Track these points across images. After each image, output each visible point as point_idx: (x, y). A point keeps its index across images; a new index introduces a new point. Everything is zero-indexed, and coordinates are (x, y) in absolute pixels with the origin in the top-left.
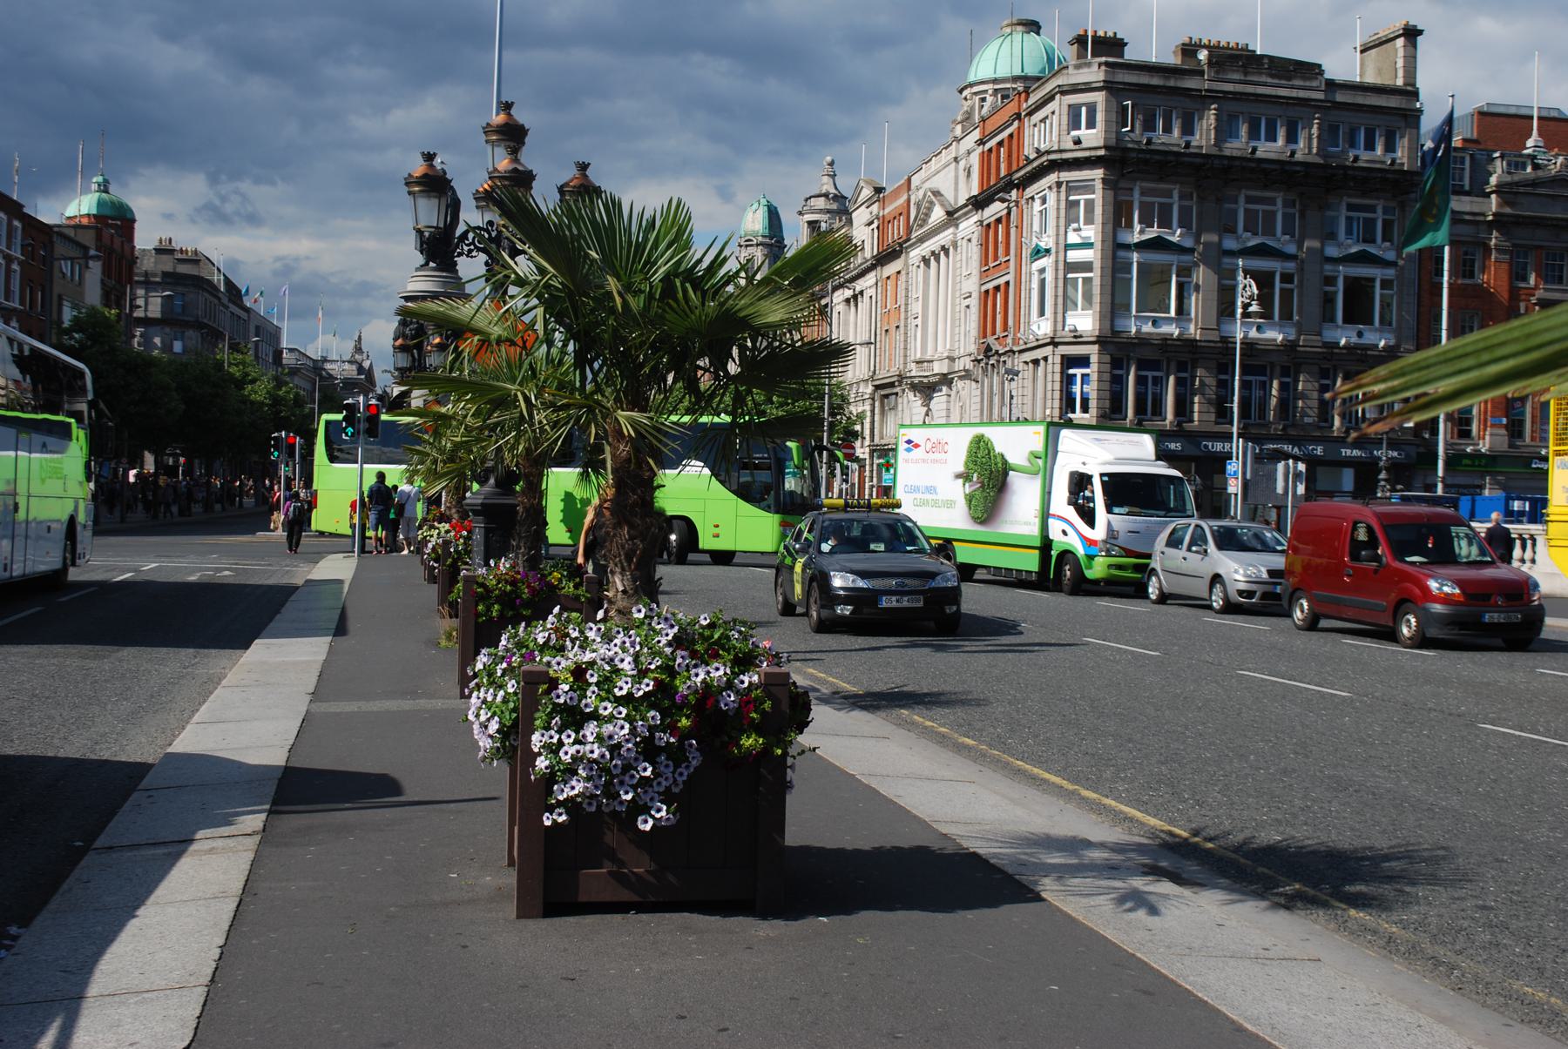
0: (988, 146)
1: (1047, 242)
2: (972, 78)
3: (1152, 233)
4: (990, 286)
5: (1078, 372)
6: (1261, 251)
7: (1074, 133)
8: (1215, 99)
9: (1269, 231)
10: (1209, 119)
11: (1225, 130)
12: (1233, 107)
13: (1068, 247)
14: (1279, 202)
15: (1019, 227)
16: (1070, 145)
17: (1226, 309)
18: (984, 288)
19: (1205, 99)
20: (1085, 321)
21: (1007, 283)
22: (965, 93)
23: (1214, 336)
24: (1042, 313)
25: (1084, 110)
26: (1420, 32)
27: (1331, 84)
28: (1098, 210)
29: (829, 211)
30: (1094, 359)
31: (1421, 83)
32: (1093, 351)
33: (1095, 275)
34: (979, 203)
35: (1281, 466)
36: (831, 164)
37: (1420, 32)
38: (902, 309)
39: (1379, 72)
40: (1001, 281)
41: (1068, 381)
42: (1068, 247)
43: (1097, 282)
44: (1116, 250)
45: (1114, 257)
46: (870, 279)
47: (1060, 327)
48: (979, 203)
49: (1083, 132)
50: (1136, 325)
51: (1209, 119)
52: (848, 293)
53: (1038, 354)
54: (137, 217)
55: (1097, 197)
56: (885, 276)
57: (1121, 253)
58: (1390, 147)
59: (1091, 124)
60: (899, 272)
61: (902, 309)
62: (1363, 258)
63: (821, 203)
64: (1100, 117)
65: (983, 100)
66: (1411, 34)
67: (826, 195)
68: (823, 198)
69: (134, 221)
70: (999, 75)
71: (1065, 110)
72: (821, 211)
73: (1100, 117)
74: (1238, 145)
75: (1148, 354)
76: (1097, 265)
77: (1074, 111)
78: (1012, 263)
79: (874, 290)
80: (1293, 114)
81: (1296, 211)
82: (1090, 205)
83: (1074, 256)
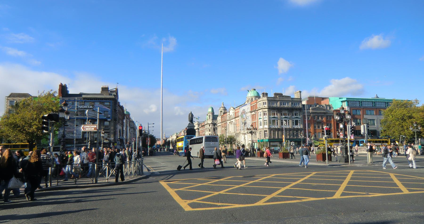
0: (252, 105)
1: (262, 117)
2: (248, 96)
3: (273, 116)
4: (253, 122)
5: (266, 132)
6: (286, 118)
7: (264, 105)
8: (279, 101)
9: (286, 115)
10: (279, 103)
11: (281, 104)
13: (264, 118)
14: (287, 112)
15: (257, 115)
17: (282, 123)
18: (252, 122)
19: (278, 101)
20: (267, 126)
21: (256, 122)
22: (247, 98)
23: (281, 128)
24: (261, 125)
25: (265, 103)
26: (301, 92)
28: (267, 114)
29: (223, 109)
30: (268, 131)
32: (268, 130)
33: (267, 121)
34: (251, 112)
35: (292, 142)
36: (223, 103)
37: (301, 92)
39: (297, 96)
40: (255, 121)
41: (265, 134)
42: (264, 118)
43: (268, 122)
44: (269, 118)
45: (269, 119)
46: (234, 120)
47: (263, 127)
48: (251, 112)
49: (265, 105)
50: (273, 127)
51: (279, 103)
52: (230, 121)
53: (261, 130)
54: (130, 114)
55: (267, 112)
57: (270, 119)
58: (299, 105)
59: (266, 104)
62: (297, 118)
63: (222, 108)
64: (267, 103)
65: (249, 99)
66: (300, 92)
67: (223, 107)
69: (130, 115)
70: (252, 96)
71: (263, 103)
72: (222, 109)
73: (267, 103)
74: (282, 106)
75: (274, 130)
76: (267, 120)
77: (264, 103)
79: (234, 122)
80: (288, 102)
81: (289, 113)
82: (266, 113)
83: (265, 119)
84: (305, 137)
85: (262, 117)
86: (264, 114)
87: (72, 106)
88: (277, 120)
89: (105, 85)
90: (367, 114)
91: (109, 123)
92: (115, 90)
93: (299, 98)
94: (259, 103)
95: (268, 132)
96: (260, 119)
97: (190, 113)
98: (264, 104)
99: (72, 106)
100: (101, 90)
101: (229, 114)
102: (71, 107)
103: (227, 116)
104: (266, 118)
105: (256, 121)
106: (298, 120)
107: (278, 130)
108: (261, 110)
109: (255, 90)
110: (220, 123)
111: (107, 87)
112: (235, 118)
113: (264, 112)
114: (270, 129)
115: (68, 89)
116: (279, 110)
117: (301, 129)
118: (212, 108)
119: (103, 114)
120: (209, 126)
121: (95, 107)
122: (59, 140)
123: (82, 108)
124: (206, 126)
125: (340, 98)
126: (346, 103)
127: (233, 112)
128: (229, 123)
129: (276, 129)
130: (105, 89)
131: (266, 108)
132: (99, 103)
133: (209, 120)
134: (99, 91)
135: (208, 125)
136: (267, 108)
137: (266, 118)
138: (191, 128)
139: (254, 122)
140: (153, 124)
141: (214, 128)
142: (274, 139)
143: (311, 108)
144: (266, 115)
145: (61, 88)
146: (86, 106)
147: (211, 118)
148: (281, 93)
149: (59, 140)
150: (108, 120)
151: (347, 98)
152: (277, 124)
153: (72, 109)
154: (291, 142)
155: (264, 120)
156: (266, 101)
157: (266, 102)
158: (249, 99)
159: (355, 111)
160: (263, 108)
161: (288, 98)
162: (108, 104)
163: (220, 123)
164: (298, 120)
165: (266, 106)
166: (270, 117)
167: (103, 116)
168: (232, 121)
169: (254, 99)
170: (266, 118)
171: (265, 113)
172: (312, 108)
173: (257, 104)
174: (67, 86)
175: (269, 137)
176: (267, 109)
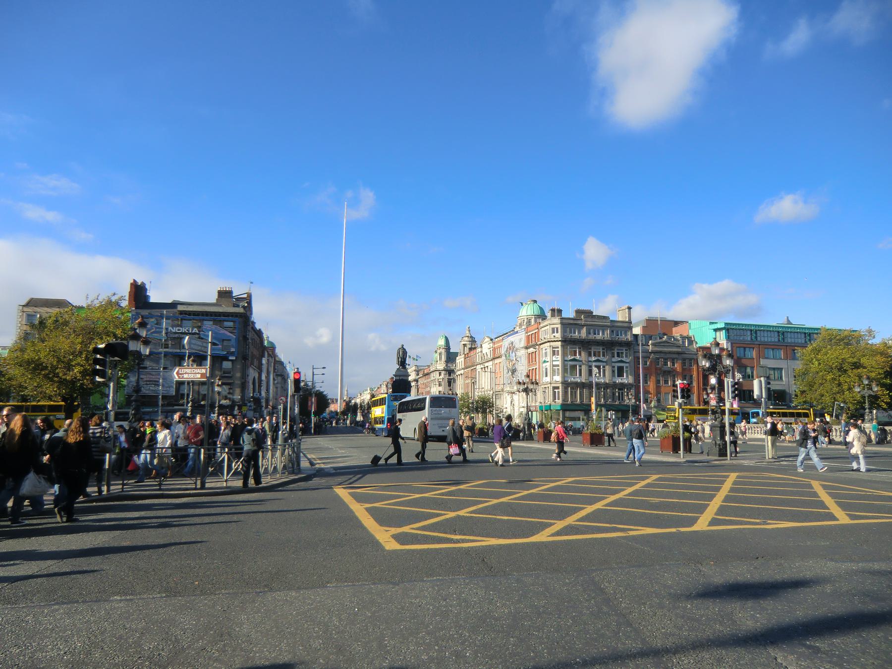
0: (528, 334)
1: (548, 359)
2: (520, 315)
3: (572, 358)
4: (531, 368)
5: (556, 390)
6: (598, 361)
7: (554, 334)
8: (585, 326)
10: (584, 330)
11: (588, 333)
12: (589, 327)
13: (553, 361)
14: (601, 349)
15: (539, 355)
16: (553, 337)
17: (590, 373)
18: (529, 369)
19: (583, 326)
20: (558, 378)
21: (536, 368)
22: (519, 318)
23: (588, 381)
24: (546, 376)
26: (631, 308)
27: (612, 321)
29: (469, 341)
30: (560, 387)
31: (632, 320)
32: (560, 385)
33: (560, 367)
35: (609, 412)
37: (631, 308)
38: (502, 372)
39: (622, 317)
40: (534, 368)
41: (554, 393)
42: (553, 361)
43: (560, 369)
44: (564, 361)
45: (564, 362)
46: (491, 363)
48: (527, 348)
49: (555, 334)
50: (571, 379)
51: (584, 330)
52: (482, 366)
53: (546, 386)
54: (277, 347)
55: (560, 349)
56: (495, 363)
57: (566, 362)
58: (626, 335)
59: (557, 332)
60: (500, 362)
61: (502, 372)
62: (622, 361)
64: (559, 331)
65: (524, 320)
66: (629, 308)
67: (468, 337)
68: (467, 338)
69: (275, 348)
70: (528, 314)
71: (551, 329)
72: (467, 341)
73: (559, 331)
74: (592, 337)
75: (573, 385)
76: (560, 365)
77: (553, 329)
78: (537, 363)
79: (491, 367)
80: (604, 328)
81: (605, 351)
82: (558, 351)
83: (555, 363)
84: (638, 403)
85: (548, 359)
86: (554, 353)
87: (156, 328)
88: (580, 366)
89: (225, 286)
90: (766, 356)
91: (233, 363)
92: (245, 296)
93: (627, 320)
94: (543, 329)
95: (560, 390)
96: (545, 362)
97: (400, 347)
98: (553, 332)
99: (156, 328)
100: (216, 296)
101: (481, 352)
102: (153, 329)
103: (477, 355)
104: (558, 360)
105: (537, 367)
106: (623, 367)
107: (582, 385)
108: (548, 344)
109: (535, 301)
110: (463, 369)
111: (230, 290)
112: (494, 359)
113: (553, 348)
114: (566, 384)
115: (148, 291)
116: (585, 345)
117: (630, 384)
118: (446, 337)
119: (220, 346)
120: (440, 375)
121: (204, 330)
122: (127, 397)
123: (176, 333)
124: (432, 375)
125: (711, 323)
126: (723, 333)
127: (489, 347)
128: (480, 370)
129: (576, 385)
130: (225, 294)
131: (557, 341)
132: (211, 323)
133: (438, 363)
134: (213, 298)
135: (438, 373)
136: (560, 341)
137: (558, 361)
138: (401, 378)
139: (533, 368)
140: (324, 368)
141: (448, 379)
142: (573, 404)
143: (650, 342)
144: (558, 355)
145: (134, 290)
146: (185, 329)
147: (444, 358)
148: (590, 311)
149: (127, 397)
150: (231, 358)
151: (726, 324)
152: (580, 375)
153: (156, 335)
154: (608, 411)
155: (554, 366)
156: (559, 326)
157: (557, 328)
158: (524, 320)
159: (742, 349)
160: (552, 340)
161: (604, 321)
162: (231, 324)
163: (463, 369)
164: (623, 367)
165: (558, 335)
166: (566, 359)
167: (219, 350)
168: (487, 367)
169: (533, 321)
170: (558, 361)
171: (556, 349)
172: (654, 342)
173: (538, 332)
174: (147, 287)
175: (563, 400)
176: (560, 342)
